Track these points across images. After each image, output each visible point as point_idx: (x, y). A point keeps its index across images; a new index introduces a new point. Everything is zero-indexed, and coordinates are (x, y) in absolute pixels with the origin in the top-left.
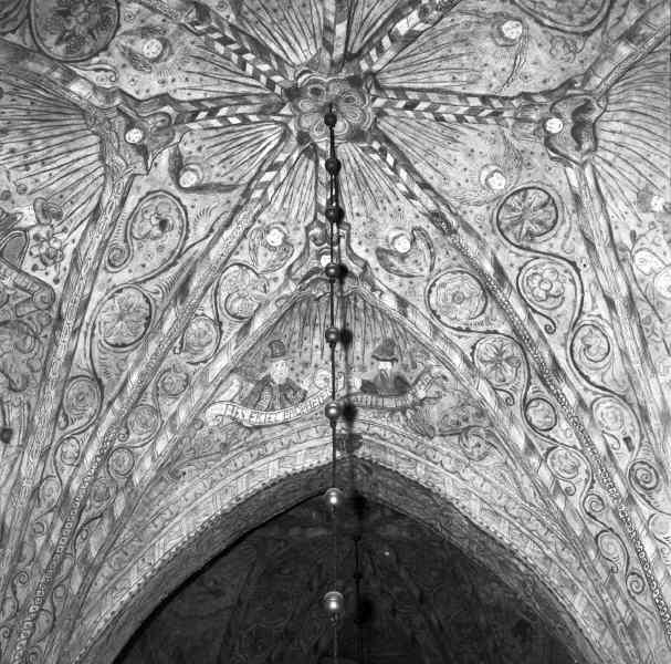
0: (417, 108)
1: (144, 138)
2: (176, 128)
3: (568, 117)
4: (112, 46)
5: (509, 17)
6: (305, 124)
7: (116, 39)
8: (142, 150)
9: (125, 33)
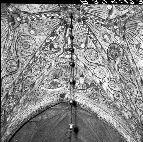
0: (51, 17)
1: (114, 26)
2: (107, 25)
3: (16, 22)
4: (112, 43)
5: (33, 35)
6: (78, 12)
7: (111, 43)
8: (116, 24)
9: (109, 43)
